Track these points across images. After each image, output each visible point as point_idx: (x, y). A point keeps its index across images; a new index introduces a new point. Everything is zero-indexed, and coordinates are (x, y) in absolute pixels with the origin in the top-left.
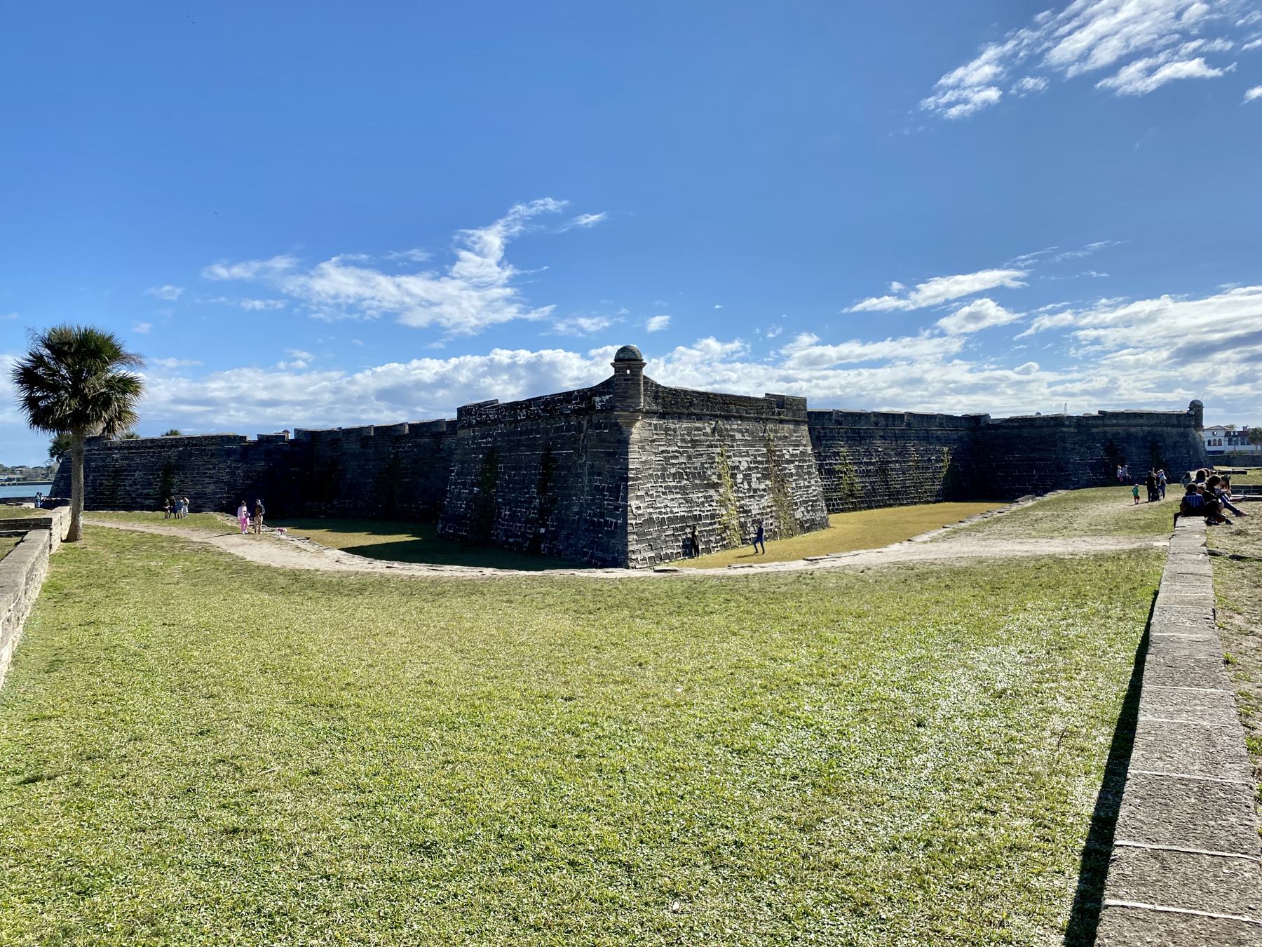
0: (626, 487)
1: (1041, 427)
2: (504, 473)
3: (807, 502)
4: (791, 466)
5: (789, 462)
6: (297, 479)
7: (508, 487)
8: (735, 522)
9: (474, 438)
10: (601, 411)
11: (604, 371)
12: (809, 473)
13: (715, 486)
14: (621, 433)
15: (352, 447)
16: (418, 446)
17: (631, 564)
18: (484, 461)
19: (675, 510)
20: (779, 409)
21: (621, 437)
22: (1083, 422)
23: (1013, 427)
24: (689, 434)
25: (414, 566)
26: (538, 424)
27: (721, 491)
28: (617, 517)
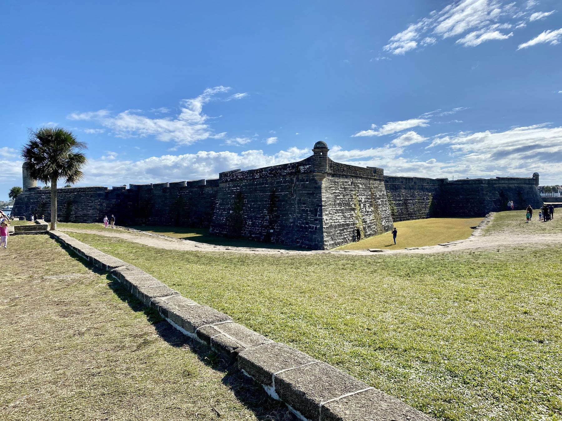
0: (321, 210)
1: (472, 184)
3: (385, 217)
4: (379, 201)
5: (379, 199)
6: (136, 207)
8: (362, 227)
10: (304, 173)
11: (307, 152)
12: (386, 204)
13: (354, 209)
14: (317, 184)
15: (159, 193)
16: (192, 192)
17: (325, 247)
19: (340, 221)
20: (374, 173)
21: (317, 186)
22: (490, 182)
23: (459, 184)
24: (343, 185)
25: (240, 248)
26: (267, 180)
27: (356, 212)
28: (316, 224)
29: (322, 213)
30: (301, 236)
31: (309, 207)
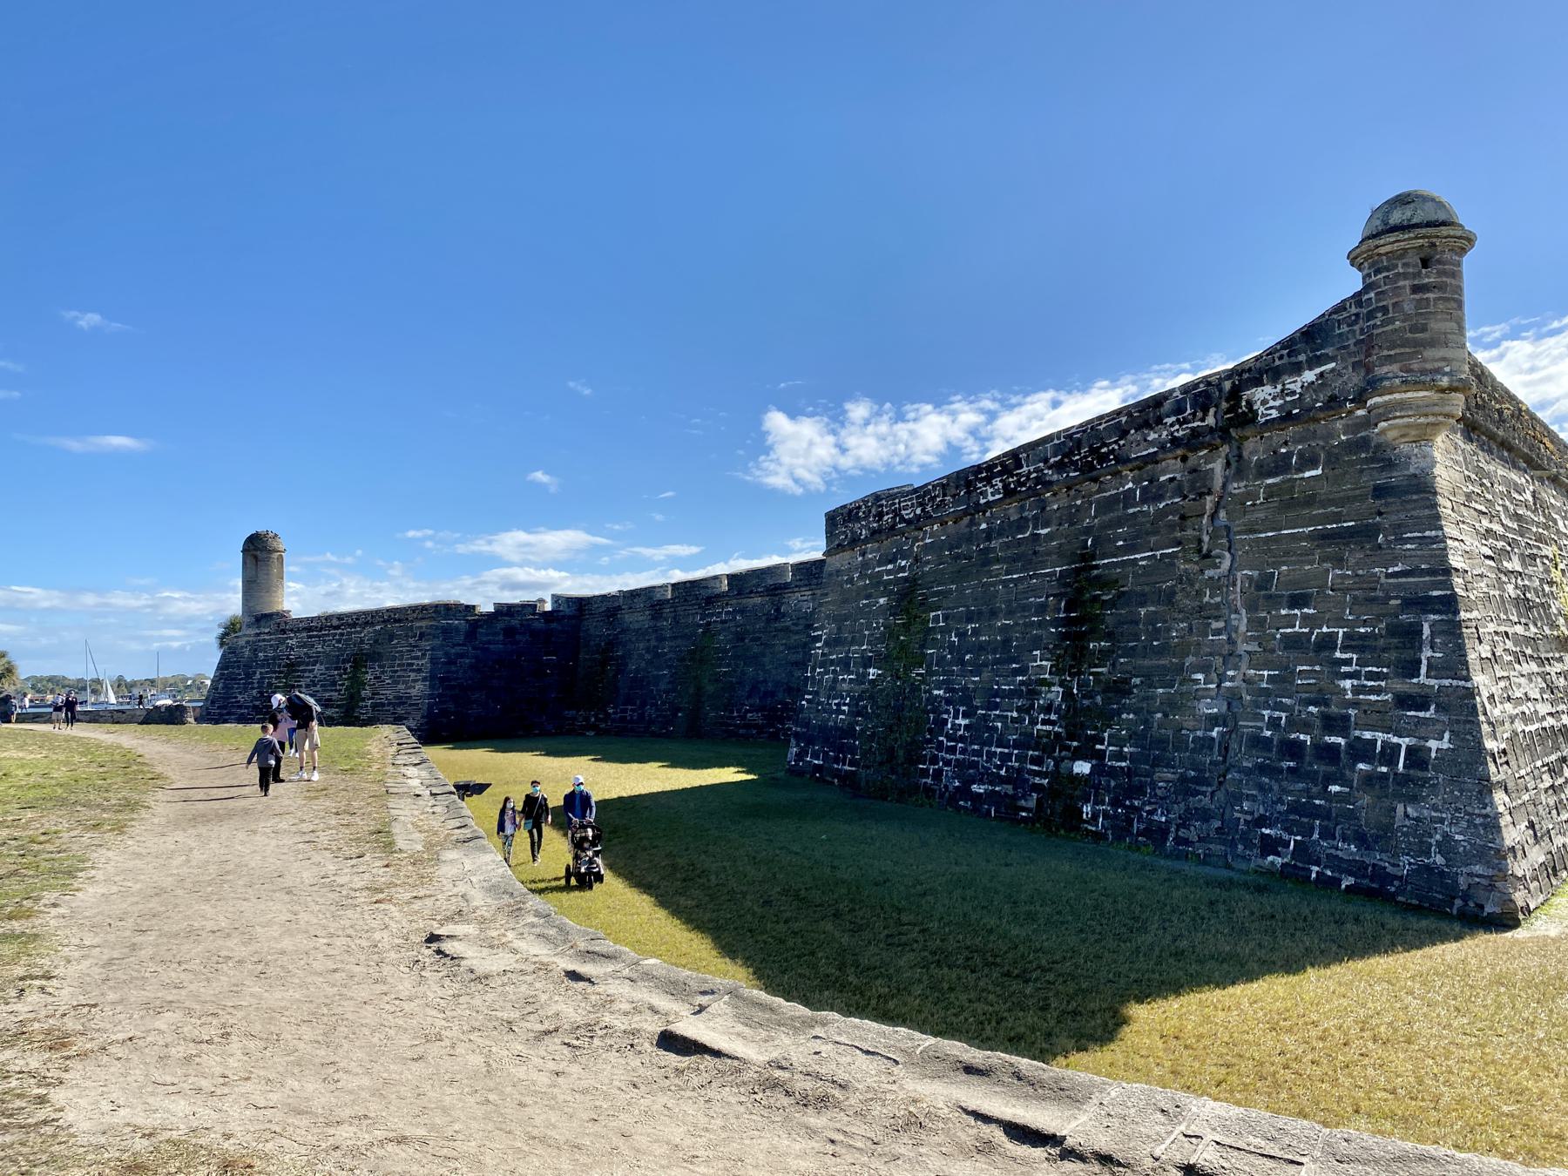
2: (946, 631)
7: (962, 662)
9: (865, 565)
10: (1287, 418)
14: (1389, 465)
18: (892, 610)
21: (1395, 478)
29: (1460, 652)
30: (1294, 808)
31: (1340, 622)
